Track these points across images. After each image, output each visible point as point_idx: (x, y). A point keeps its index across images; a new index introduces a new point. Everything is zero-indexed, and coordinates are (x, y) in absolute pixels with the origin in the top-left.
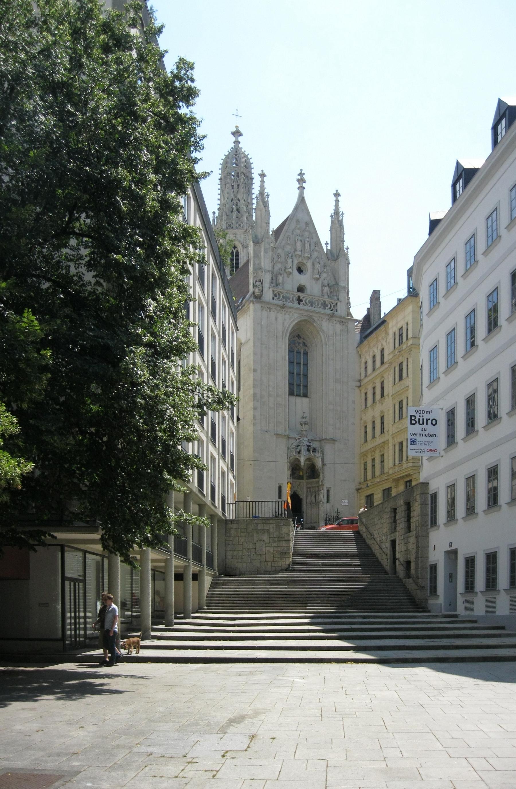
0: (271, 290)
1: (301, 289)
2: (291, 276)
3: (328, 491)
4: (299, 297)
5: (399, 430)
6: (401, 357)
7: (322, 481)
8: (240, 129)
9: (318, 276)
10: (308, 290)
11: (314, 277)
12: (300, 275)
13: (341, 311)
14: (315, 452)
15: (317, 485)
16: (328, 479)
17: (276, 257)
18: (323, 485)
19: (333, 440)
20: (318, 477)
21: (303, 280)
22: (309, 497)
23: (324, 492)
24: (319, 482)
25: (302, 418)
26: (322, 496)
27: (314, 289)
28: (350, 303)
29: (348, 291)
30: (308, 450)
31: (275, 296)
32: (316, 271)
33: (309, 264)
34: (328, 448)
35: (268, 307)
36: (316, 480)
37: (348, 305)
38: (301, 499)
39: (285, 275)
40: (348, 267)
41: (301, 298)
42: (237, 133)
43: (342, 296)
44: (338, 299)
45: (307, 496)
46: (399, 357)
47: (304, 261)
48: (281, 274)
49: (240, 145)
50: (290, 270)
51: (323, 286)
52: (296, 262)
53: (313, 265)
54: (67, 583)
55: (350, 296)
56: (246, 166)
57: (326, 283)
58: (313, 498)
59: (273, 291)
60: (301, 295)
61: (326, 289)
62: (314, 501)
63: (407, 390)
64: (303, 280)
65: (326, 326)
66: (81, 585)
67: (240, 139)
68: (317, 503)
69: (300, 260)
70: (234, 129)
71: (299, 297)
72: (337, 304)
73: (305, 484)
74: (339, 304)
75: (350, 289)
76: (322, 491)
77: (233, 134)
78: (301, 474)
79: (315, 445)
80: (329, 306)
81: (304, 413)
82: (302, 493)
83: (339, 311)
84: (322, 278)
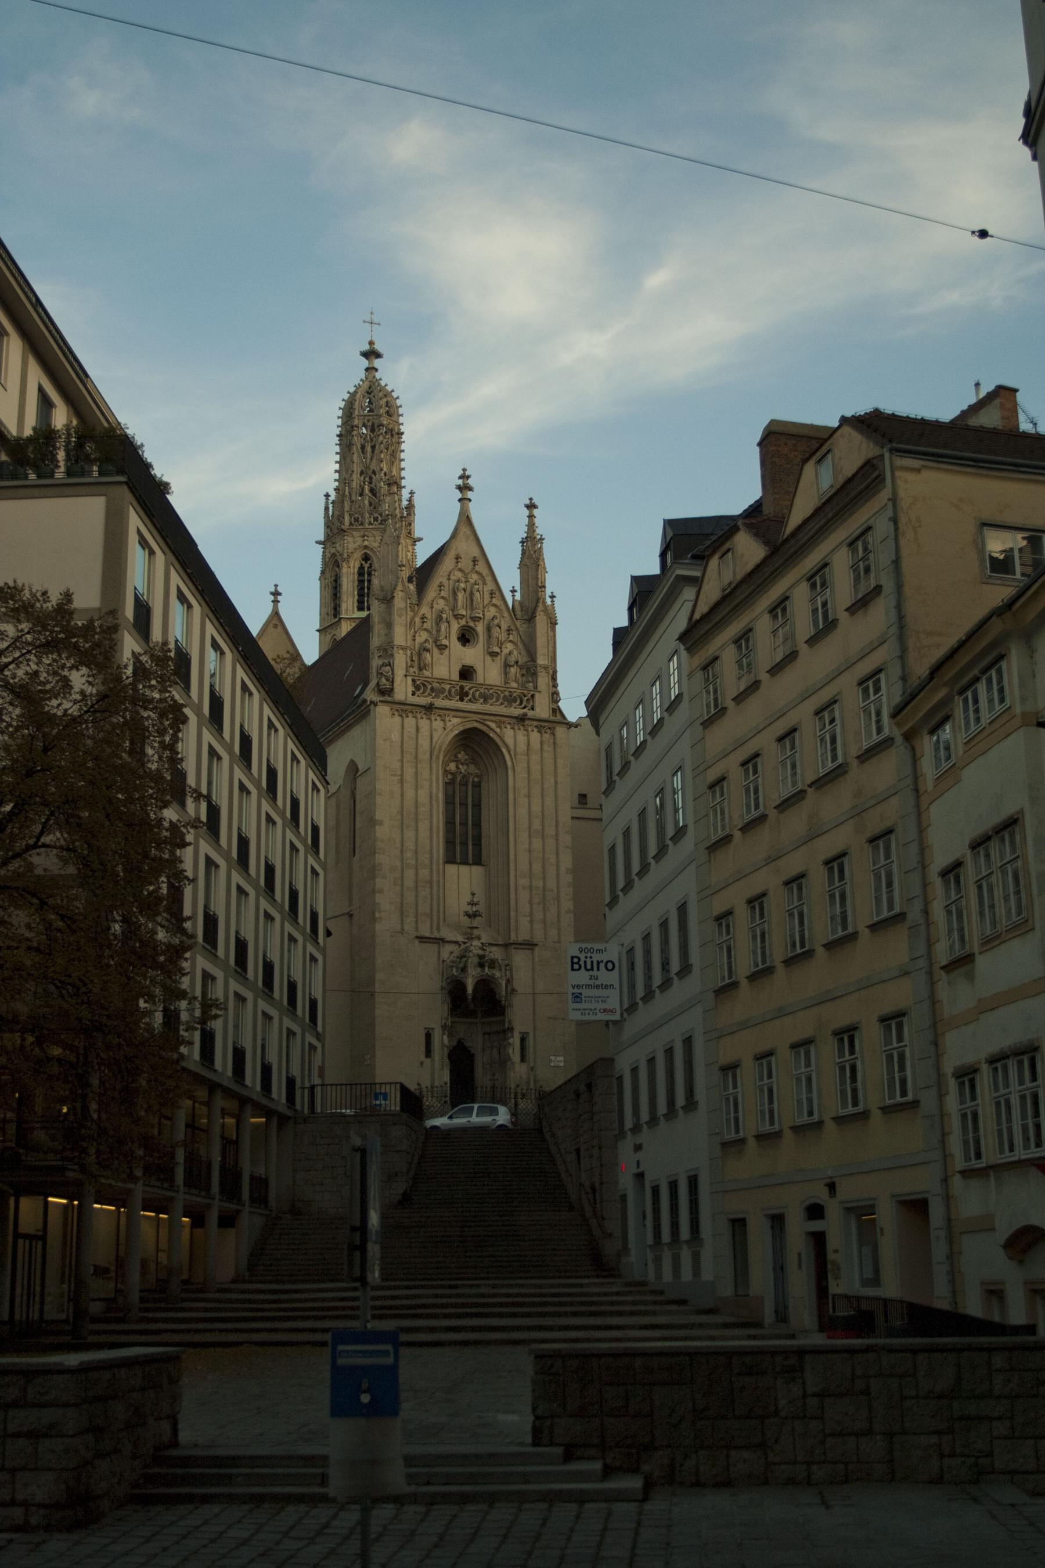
0: (409, 679)
1: (466, 673)
2: (446, 652)
3: (523, 1040)
4: (462, 688)
7: (510, 1021)
8: (378, 347)
9: (496, 649)
10: (480, 678)
12: (465, 649)
13: (542, 710)
14: (494, 968)
16: (520, 1015)
17: (417, 620)
18: (511, 1029)
19: (529, 945)
20: (503, 1014)
21: (472, 655)
23: (516, 1041)
24: (504, 1021)
26: (511, 1051)
27: (490, 673)
28: (558, 694)
29: (555, 672)
30: (481, 965)
31: (417, 688)
32: (494, 641)
33: (480, 628)
34: (520, 959)
35: (403, 708)
36: (502, 1018)
37: (555, 697)
38: (473, 1055)
39: (436, 651)
40: (554, 630)
41: (466, 689)
42: (371, 354)
43: (543, 680)
44: (536, 687)
45: (483, 1050)
47: (472, 624)
48: (428, 650)
49: (378, 375)
50: (445, 642)
51: (507, 665)
52: (455, 627)
53: (489, 629)
54: (20, 1242)
55: (559, 681)
56: (388, 412)
57: (512, 659)
59: (413, 680)
60: (467, 685)
61: (513, 670)
64: (472, 655)
65: (512, 738)
66: (40, 1243)
67: (377, 363)
68: (504, 1062)
69: (463, 622)
70: (366, 347)
71: (462, 688)
72: (533, 696)
74: (537, 695)
75: (558, 669)
76: (511, 1041)
77: (366, 355)
79: (496, 953)
80: (518, 702)
82: (476, 1043)
83: (537, 709)
84: (505, 651)
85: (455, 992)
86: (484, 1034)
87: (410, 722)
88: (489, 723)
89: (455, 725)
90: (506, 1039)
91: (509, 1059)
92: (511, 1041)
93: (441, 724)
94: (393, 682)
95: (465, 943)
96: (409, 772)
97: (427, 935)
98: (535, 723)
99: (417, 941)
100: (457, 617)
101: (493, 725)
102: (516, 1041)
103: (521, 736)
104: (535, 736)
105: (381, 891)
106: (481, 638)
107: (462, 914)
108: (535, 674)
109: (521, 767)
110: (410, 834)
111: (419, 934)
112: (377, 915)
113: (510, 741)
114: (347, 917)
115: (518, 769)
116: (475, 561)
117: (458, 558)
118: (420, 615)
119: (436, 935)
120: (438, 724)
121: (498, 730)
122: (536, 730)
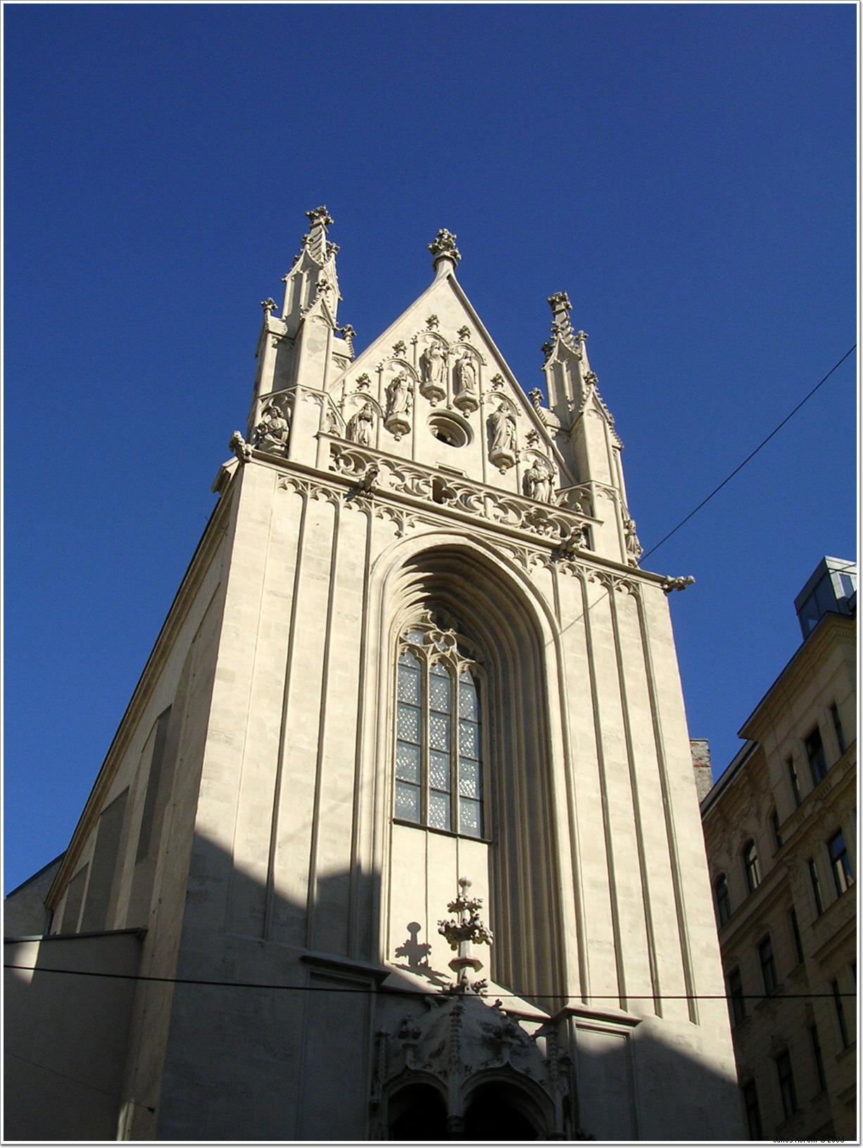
0: (326, 443)
6: (830, 818)
11: (495, 453)
25: (457, 907)
35: (305, 480)
53: (492, 424)
72: (587, 531)
74: (595, 526)
81: (463, 883)
87: (320, 509)
88: (499, 548)
89: (424, 535)
93: (395, 527)
94: (288, 441)
96: (312, 594)
100: (431, 393)
101: (508, 554)
109: (572, 640)
115: (565, 640)
116: (463, 332)
117: (431, 322)
120: (383, 526)
121: (518, 563)
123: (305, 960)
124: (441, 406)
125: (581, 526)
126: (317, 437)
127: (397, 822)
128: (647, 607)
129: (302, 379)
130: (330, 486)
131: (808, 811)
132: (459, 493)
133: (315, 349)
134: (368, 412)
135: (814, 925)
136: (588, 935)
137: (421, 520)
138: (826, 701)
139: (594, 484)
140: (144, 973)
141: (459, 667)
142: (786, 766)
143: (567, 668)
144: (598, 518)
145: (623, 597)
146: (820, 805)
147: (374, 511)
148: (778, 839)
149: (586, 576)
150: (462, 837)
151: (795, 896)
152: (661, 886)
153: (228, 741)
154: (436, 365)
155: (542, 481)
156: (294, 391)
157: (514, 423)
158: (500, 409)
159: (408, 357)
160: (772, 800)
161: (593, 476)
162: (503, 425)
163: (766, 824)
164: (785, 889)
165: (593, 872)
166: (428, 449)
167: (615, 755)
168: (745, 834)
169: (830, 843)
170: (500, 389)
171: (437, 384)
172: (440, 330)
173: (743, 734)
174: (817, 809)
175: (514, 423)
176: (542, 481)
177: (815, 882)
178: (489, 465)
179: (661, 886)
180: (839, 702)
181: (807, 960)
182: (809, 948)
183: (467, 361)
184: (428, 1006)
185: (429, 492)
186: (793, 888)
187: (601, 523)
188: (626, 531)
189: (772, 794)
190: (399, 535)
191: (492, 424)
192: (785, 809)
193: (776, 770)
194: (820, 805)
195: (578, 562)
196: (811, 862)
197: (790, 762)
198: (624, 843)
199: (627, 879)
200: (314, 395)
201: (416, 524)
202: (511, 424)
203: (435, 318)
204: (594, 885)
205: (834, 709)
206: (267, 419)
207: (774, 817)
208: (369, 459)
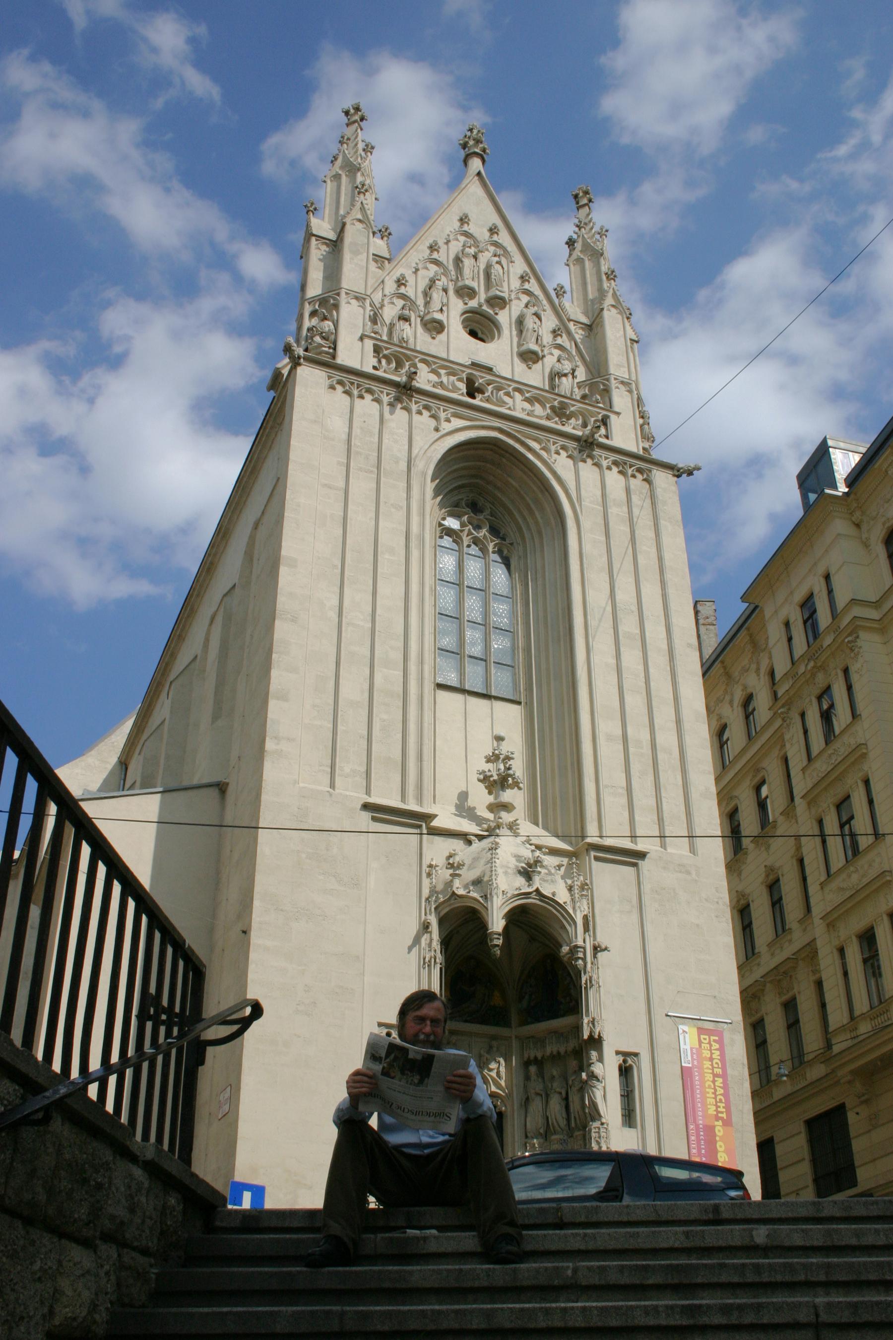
0: (369, 344)
2: (442, 337)
3: (625, 1072)
5: (848, 894)
6: (820, 677)
11: (524, 348)
15: (572, 1044)
18: (596, 1042)
22: (537, 1105)
25: (493, 758)
33: (504, 318)
35: (351, 379)
43: (621, 400)
46: (813, 675)
53: (520, 322)
58: (556, 1105)
62: (563, 1123)
63: (864, 756)
72: (605, 421)
73: (515, 1044)
74: (613, 417)
78: (497, 1000)
81: (499, 739)
85: (460, 925)
86: (527, 1064)
87: (366, 407)
89: (457, 430)
90: (583, 1064)
91: (595, 1115)
92: (597, 1069)
93: (433, 423)
94: (335, 343)
95: (481, 838)
96: (362, 486)
97: (394, 802)
98: (614, 457)
99: (366, 815)
102: (607, 1069)
103: (587, 470)
104: (613, 478)
105: (283, 697)
106: (506, 332)
107: (474, 777)
108: (607, 391)
109: (591, 522)
110: (357, 597)
111: (372, 800)
112: (269, 745)
113: (568, 475)
114: (214, 793)
115: (585, 524)
116: (493, 230)
117: (464, 220)
118: (397, 274)
119: (412, 806)
120: (424, 421)
121: (544, 454)
122: (615, 469)
123: (366, 807)
124: (473, 304)
125: (600, 417)
126: (361, 339)
127: (440, 686)
128: (659, 492)
129: (346, 284)
130: (375, 386)
131: (802, 669)
132: (490, 388)
133: (356, 253)
134: (406, 312)
135: (803, 770)
136: (604, 780)
137: (456, 415)
138: (821, 570)
139: (612, 377)
140: (228, 820)
141: (491, 547)
142: (783, 629)
143: (587, 548)
144: (616, 409)
145: (637, 483)
146: (812, 664)
147: (414, 407)
148: (775, 694)
149: (605, 463)
150: (497, 698)
151: (788, 745)
152: (667, 738)
153: (294, 620)
154: (468, 263)
155: (565, 375)
156: (338, 294)
157: (540, 319)
158: (526, 306)
159: (441, 256)
160: (770, 658)
161: (612, 370)
162: (530, 322)
163: (764, 680)
164: (779, 740)
165: (608, 727)
166: (459, 346)
167: (628, 625)
168: (745, 688)
169: (819, 698)
170: (527, 286)
171: (468, 282)
172: (471, 228)
173: (744, 598)
174: (809, 668)
175: (540, 319)
176: (565, 375)
177: (806, 732)
178: (516, 360)
179: (667, 738)
180: (832, 571)
181: (797, 800)
182: (798, 791)
183: (496, 259)
184: (469, 843)
185: (463, 387)
186: (787, 737)
187: (618, 414)
188: (641, 421)
189: (770, 653)
190: (437, 430)
191: (520, 322)
192: (782, 667)
193: (775, 633)
194: (812, 664)
195: (597, 452)
196: (803, 715)
197: (787, 624)
198: (635, 702)
199: (639, 733)
200: (357, 298)
201: (452, 419)
202: (537, 320)
203: (466, 217)
204: (610, 738)
205: (827, 577)
206: (315, 321)
207: (772, 674)
208: (408, 358)
